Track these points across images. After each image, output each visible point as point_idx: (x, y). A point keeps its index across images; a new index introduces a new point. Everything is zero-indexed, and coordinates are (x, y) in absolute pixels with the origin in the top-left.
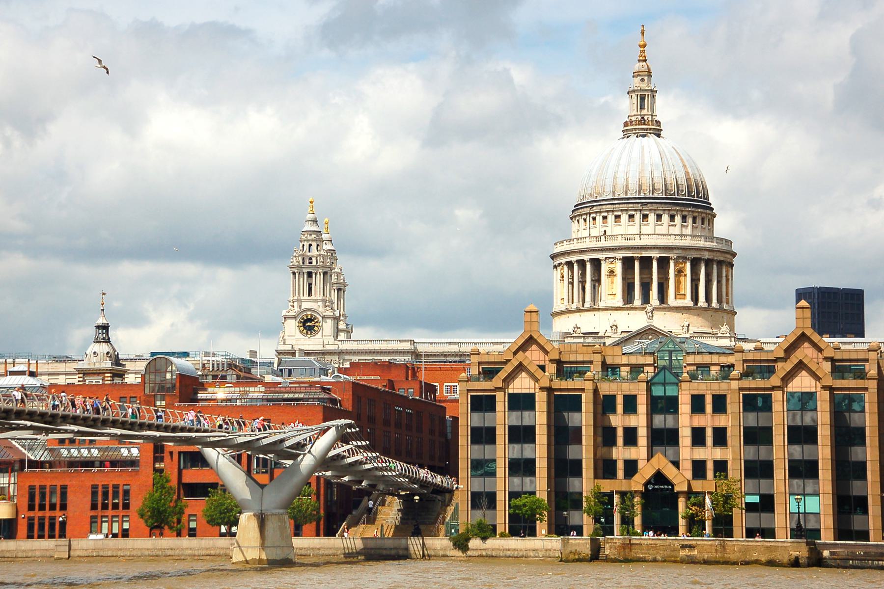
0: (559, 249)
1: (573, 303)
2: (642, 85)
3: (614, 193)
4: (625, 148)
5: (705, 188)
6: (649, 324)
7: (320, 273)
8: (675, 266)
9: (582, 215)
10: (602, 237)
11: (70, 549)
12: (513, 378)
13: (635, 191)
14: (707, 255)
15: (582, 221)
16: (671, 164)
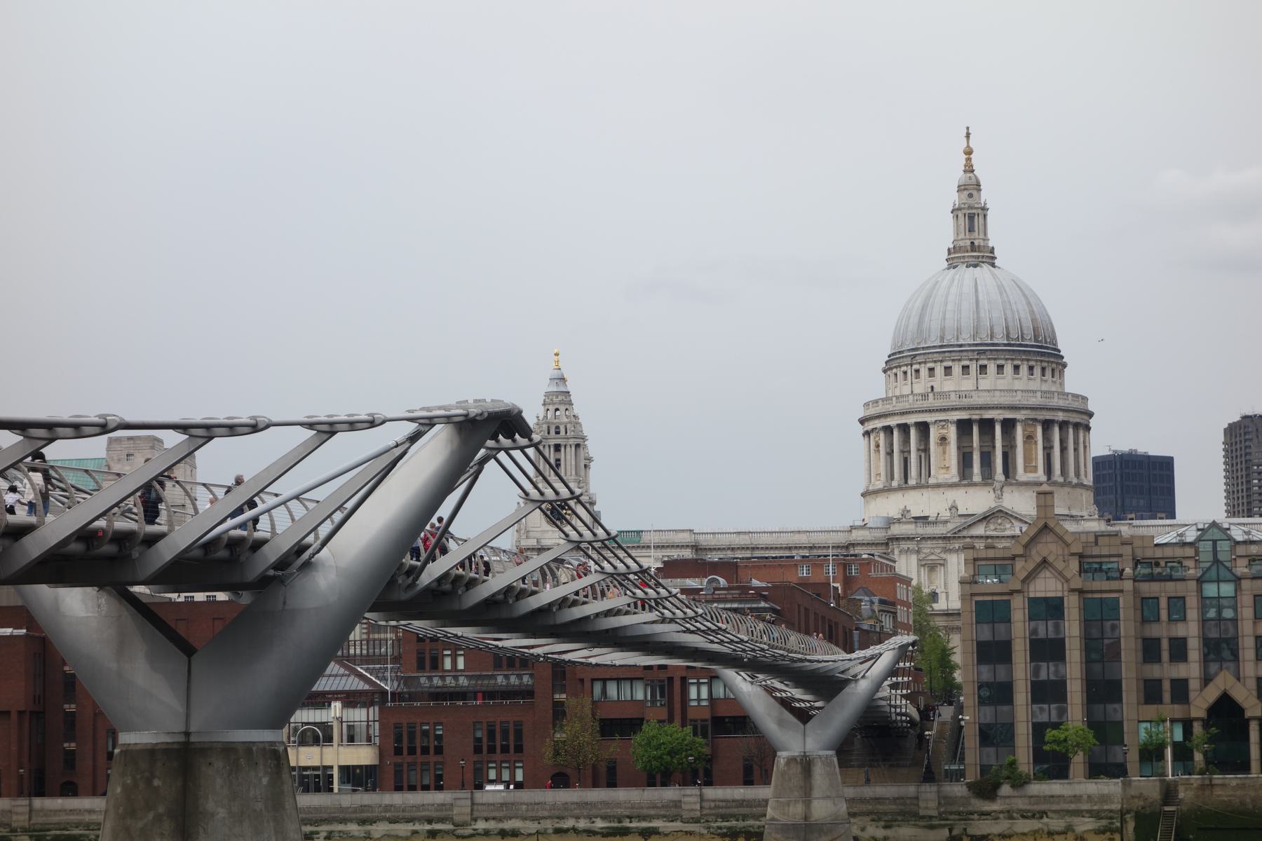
0: (873, 411)
1: (892, 478)
2: (969, 202)
3: (942, 338)
4: (953, 280)
5: (1053, 331)
6: (998, 504)
7: (571, 446)
8: (1024, 430)
9: (900, 367)
10: (929, 394)
11: (473, 804)
12: (1034, 578)
13: (969, 335)
14: (1061, 416)
15: (900, 375)
16: (1012, 302)
